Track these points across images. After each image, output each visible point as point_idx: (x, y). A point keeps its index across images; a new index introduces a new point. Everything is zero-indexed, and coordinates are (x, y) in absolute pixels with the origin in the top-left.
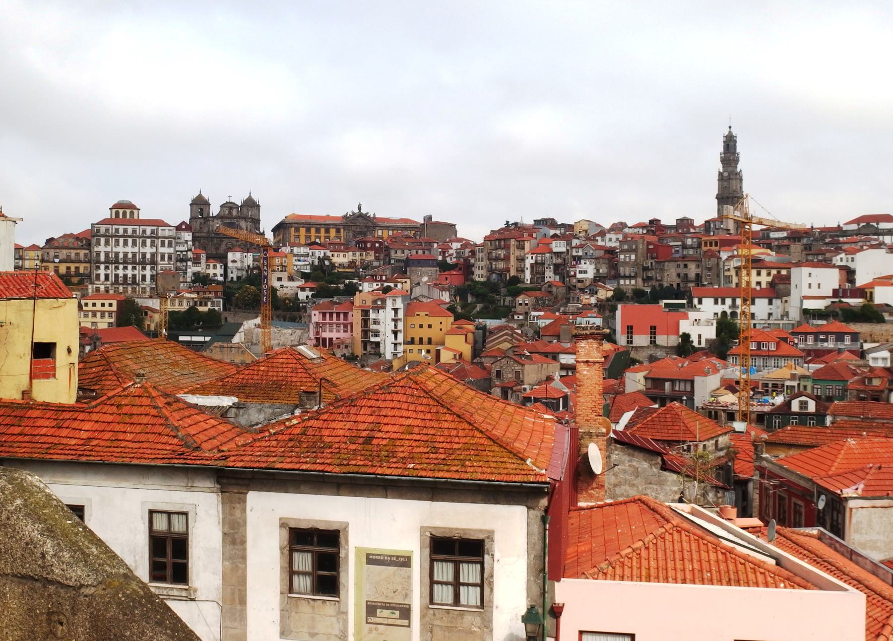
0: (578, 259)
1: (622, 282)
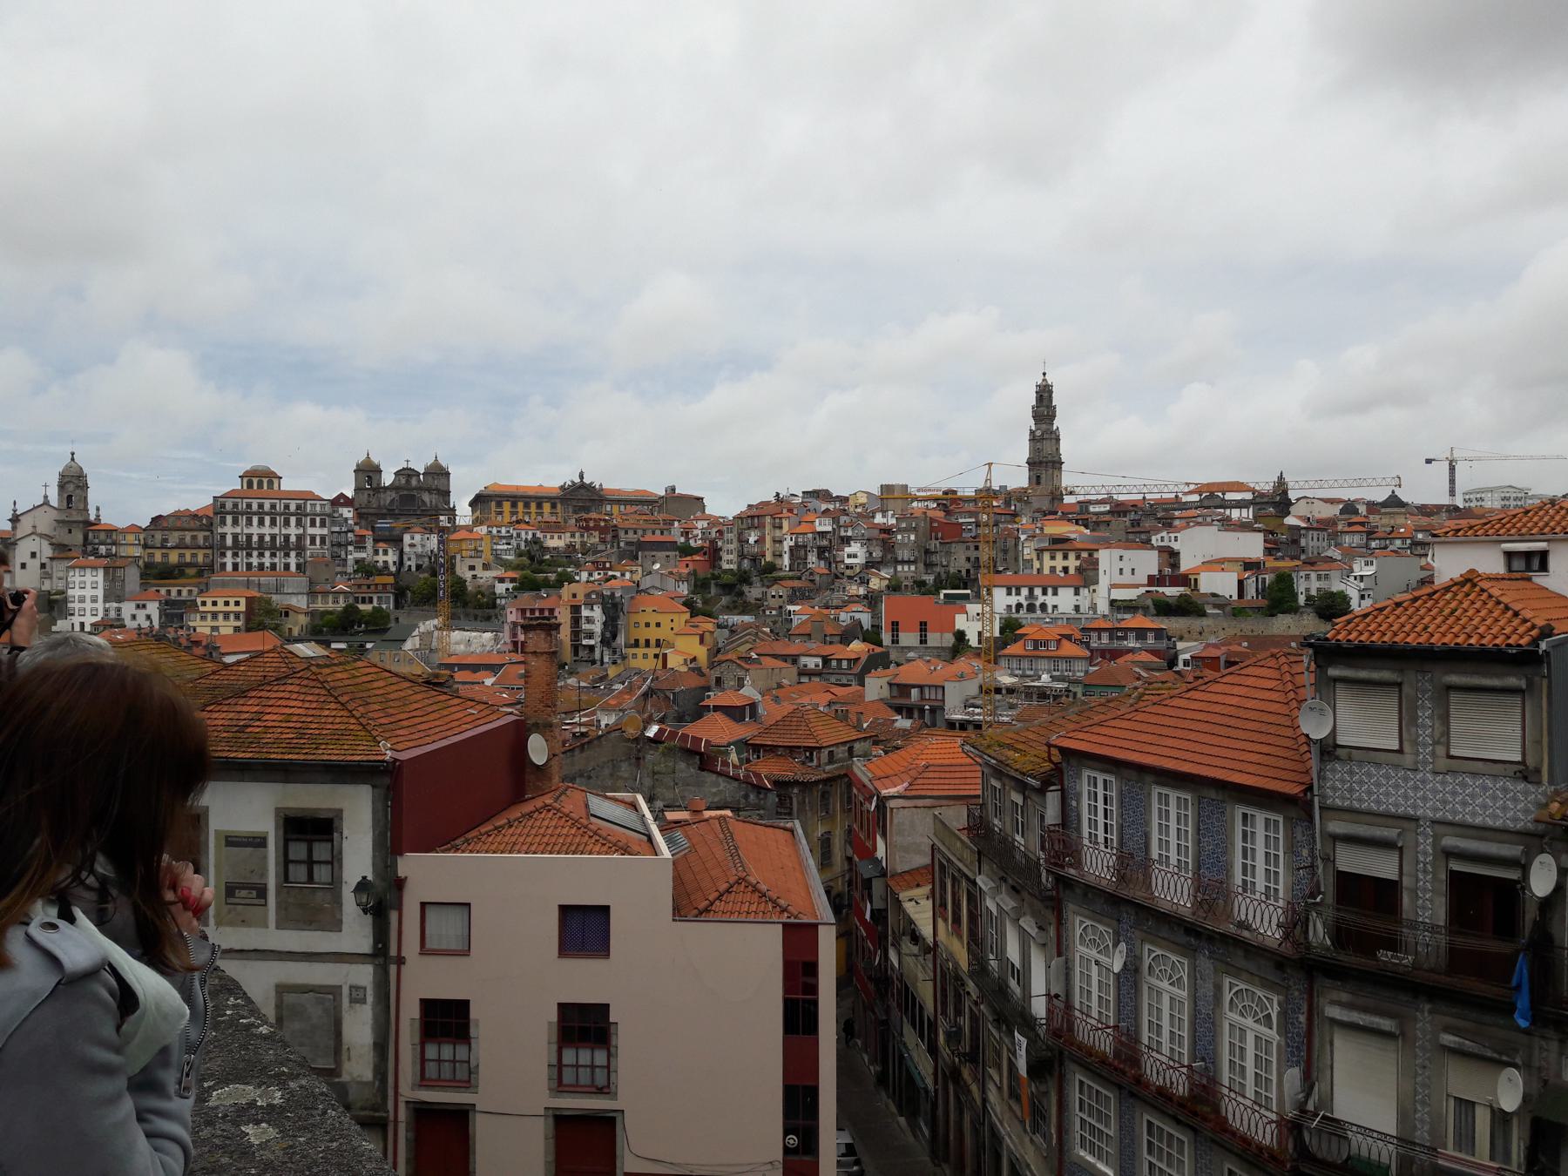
1: (899, 568)
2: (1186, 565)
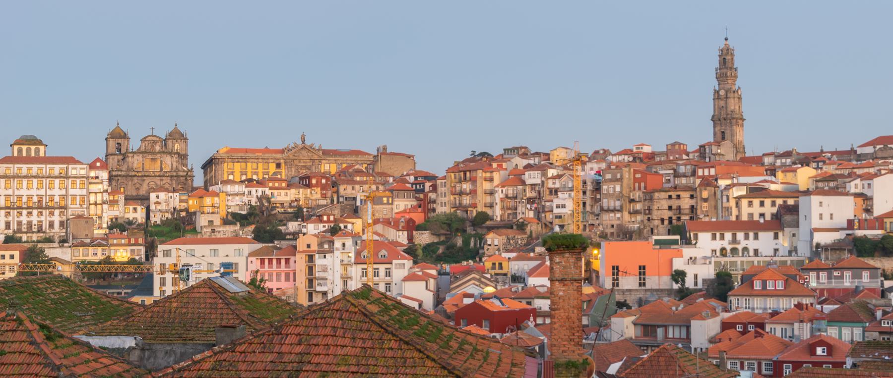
0: (555, 192)
2: (878, 211)
